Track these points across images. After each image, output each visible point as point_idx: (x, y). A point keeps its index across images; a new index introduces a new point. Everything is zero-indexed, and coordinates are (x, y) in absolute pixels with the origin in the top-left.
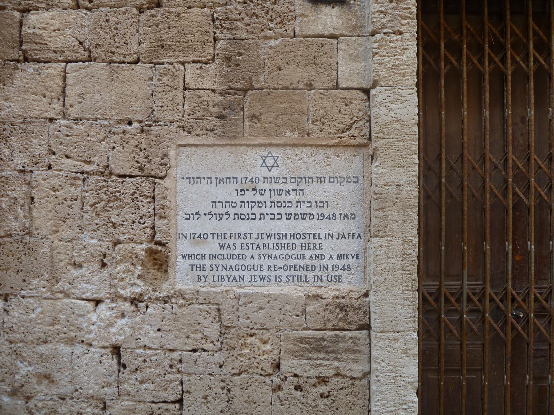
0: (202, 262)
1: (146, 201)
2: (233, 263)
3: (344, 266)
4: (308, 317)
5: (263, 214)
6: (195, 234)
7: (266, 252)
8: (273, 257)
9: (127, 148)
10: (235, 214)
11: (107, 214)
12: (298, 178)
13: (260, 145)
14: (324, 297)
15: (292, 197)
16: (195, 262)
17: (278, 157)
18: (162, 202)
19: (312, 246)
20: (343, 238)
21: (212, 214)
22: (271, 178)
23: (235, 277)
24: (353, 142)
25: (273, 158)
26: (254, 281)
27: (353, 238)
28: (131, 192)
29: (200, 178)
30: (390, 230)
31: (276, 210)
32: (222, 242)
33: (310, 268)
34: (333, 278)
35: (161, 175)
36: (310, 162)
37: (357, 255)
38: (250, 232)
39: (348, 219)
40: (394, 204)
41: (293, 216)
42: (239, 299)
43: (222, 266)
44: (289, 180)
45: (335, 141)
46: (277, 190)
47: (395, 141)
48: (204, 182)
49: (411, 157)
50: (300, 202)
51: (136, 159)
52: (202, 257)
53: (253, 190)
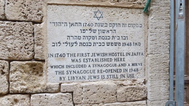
0: (62, 70)
1: (29, 36)
2: (79, 69)
3: (135, 69)
4: (118, 96)
6: (58, 54)
7: (97, 63)
8: (100, 66)
9: (17, 4)
10: (80, 43)
11: (4, 43)
12: (113, 24)
13: (93, 6)
15: (110, 34)
16: (58, 70)
18: (39, 36)
19: (120, 59)
20: (135, 55)
21: (67, 43)
24: (140, 6)
26: (91, 79)
27: (139, 55)
28: (20, 30)
29: (60, 23)
31: (102, 41)
32: (73, 58)
33: (119, 71)
36: (121, 16)
41: (110, 44)
43: (73, 71)
45: (131, 5)
46: (102, 30)
47: (160, 7)
49: (167, 15)
50: (114, 37)
51: (22, 11)
52: (62, 67)
53: (90, 30)
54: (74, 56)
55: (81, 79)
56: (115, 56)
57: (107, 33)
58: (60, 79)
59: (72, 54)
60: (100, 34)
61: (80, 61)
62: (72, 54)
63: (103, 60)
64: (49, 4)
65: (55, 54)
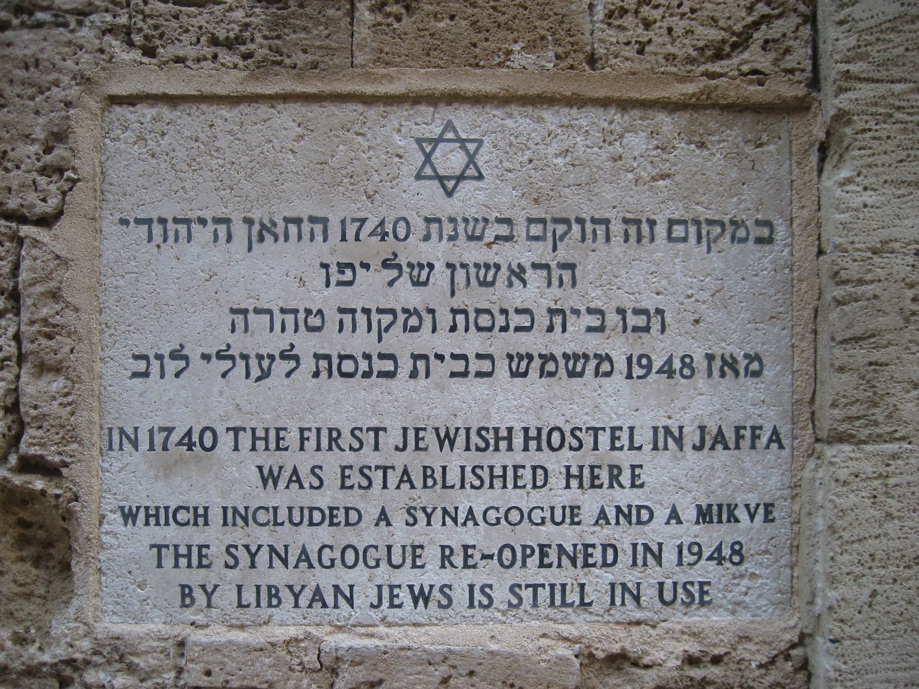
0: (196, 536)
2: (312, 538)
3: (719, 549)
5: (425, 357)
6: (170, 430)
8: (461, 517)
10: (317, 357)
12: (556, 221)
14: (646, 660)
15: (534, 294)
16: (170, 534)
17: (480, 142)
18: (45, 312)
20: (719, 447)
21: (232, 358)
22: (452, 220)
23: (318, 591)
24: (754, 92)
25: (463, 147)
26: (392, 606)
27: (753, 447)
29: (187, 221)
30: (889, 416)
31: (472, 343)
32: (270, 460)
34: (680, 590)
35: (41, 208)
37: (767, 506)
38: (375, 423)
39: (737, 373)
40: (907, 320)
41: (536, 363)
42: (334, 672)
43: (272, 549)
44: (520, 230)
45: (690, 88)
46: (477, 266)
48: (202, 234)
50: (562, 312)
52: (196, 516)
53: (386, 264)
54: (278, 448)
55: (325, 605)
56: (571, 448)
57: (511, 285)
58: (184, 596)
59: (260, 433)
60: (457, 293)
61: (316, 483)
62: (260, 433)
63: (479, 477)
64: (115, 100)
65: (151, 431)
